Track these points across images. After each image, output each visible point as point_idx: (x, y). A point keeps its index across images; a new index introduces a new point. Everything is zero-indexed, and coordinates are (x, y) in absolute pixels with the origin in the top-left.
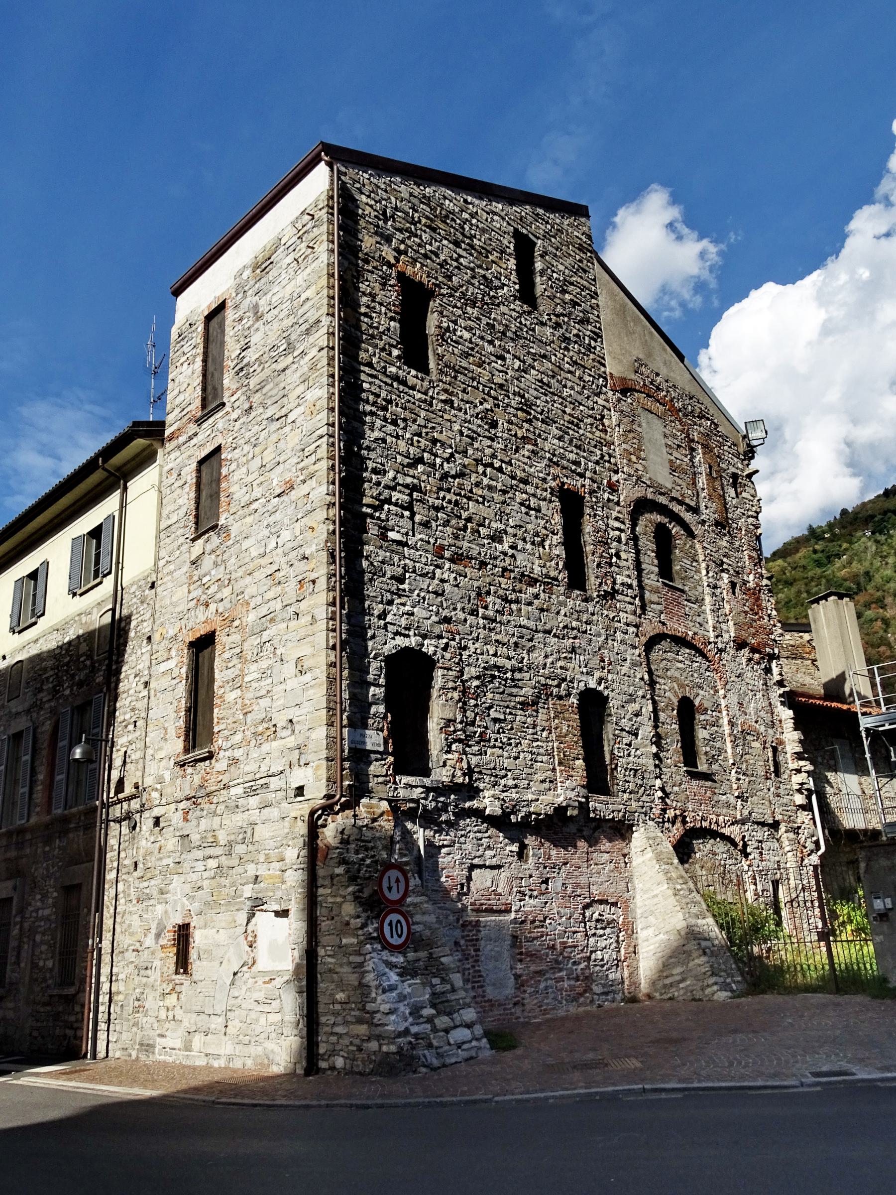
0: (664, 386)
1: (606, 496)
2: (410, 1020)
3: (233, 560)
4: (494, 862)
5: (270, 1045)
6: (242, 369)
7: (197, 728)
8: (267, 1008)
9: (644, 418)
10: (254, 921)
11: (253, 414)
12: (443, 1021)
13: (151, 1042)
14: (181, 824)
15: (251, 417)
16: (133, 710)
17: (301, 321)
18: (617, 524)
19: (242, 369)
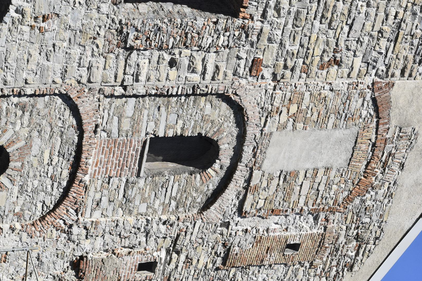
0: (390, 177)
1: (244, 55)
9: (345, 134)
18: (210, 69)
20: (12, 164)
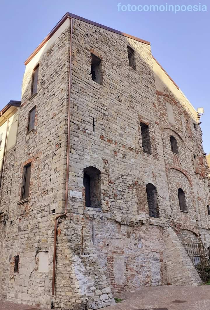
2: (87, 291)
3: (38, 140)
4: (119, 237)
5: (41, 298)
6: (42, 83)
7: (25, 193)
8: (40, 285)
10: (38, 255)
11: (45, 95)
12: (98, 292)
13: (6, 295)
14: (18, 223)
15: (45, 96)
16: (7, 188)
17: (60, 65)
19: (42, 83)
20: (181, 188)
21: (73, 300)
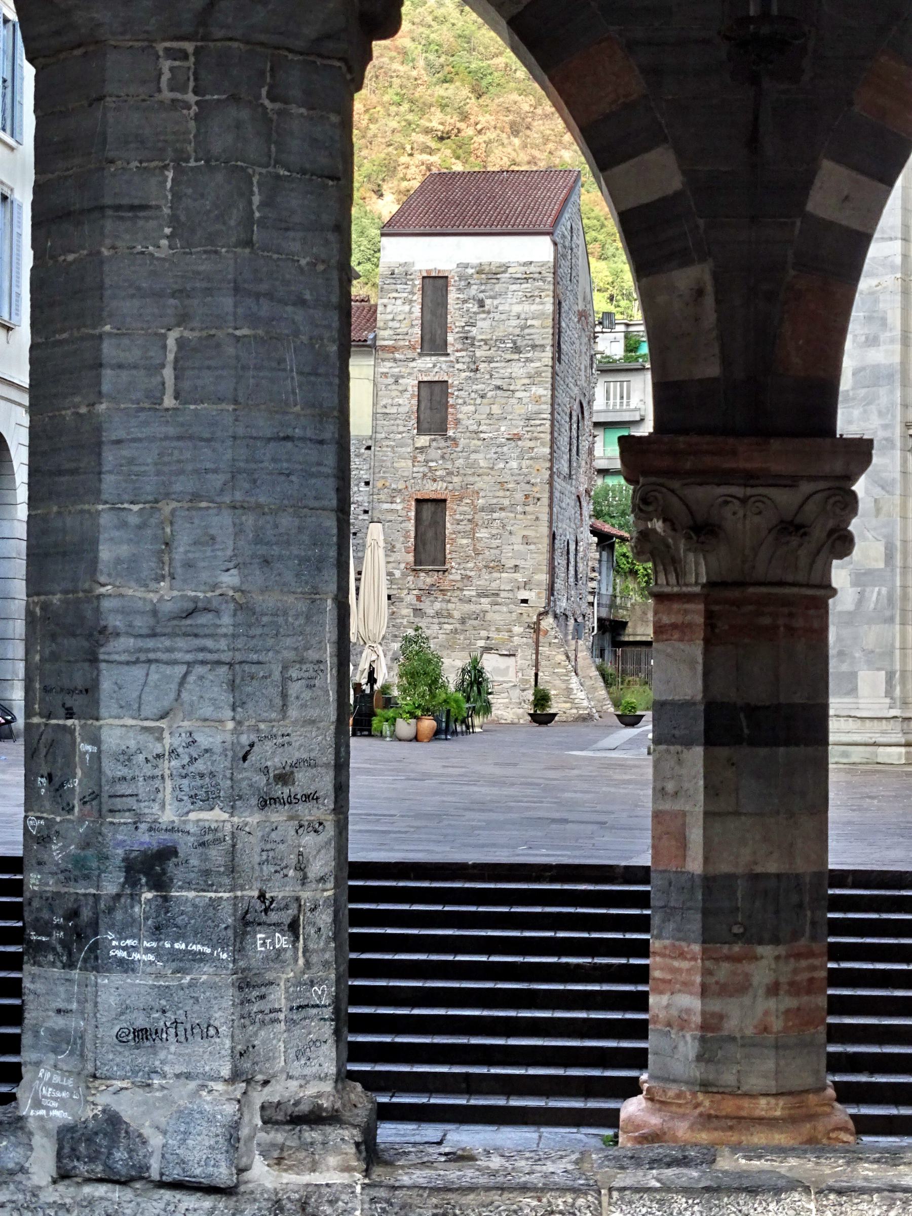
3: (461, 461)
14: (414, 601)
19: (467, 338)
21: (575, 711)
